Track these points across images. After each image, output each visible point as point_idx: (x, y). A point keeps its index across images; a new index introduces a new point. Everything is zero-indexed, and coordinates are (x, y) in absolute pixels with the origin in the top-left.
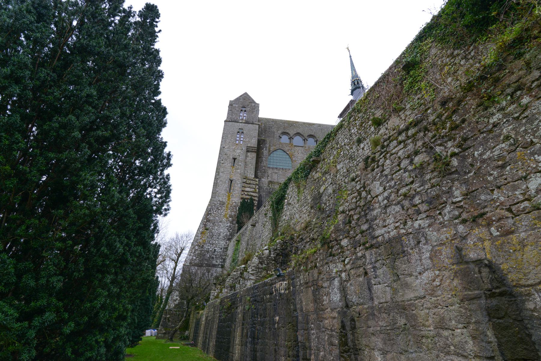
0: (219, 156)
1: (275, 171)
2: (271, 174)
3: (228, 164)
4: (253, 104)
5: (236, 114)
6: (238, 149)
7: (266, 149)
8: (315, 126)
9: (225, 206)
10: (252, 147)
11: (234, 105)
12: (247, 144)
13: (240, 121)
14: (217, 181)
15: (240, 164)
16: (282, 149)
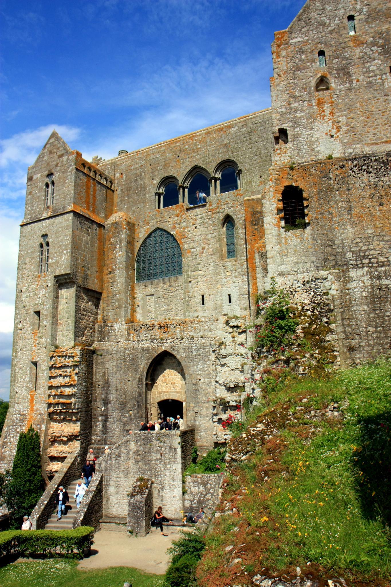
0: (16, 314)
1: (150, 289)
2: (142, 300)
3: (28, 330)
5: (38, 197)
6: (41, 288)
7: (120, 247)
8: (232, 130)
9: (26, 423)
10: (62, 275)
11: (35, 178)
12: (55, 270)
13: (45, 215)
14: (15, 370)
15: (45, 323)
16: (161, 226)
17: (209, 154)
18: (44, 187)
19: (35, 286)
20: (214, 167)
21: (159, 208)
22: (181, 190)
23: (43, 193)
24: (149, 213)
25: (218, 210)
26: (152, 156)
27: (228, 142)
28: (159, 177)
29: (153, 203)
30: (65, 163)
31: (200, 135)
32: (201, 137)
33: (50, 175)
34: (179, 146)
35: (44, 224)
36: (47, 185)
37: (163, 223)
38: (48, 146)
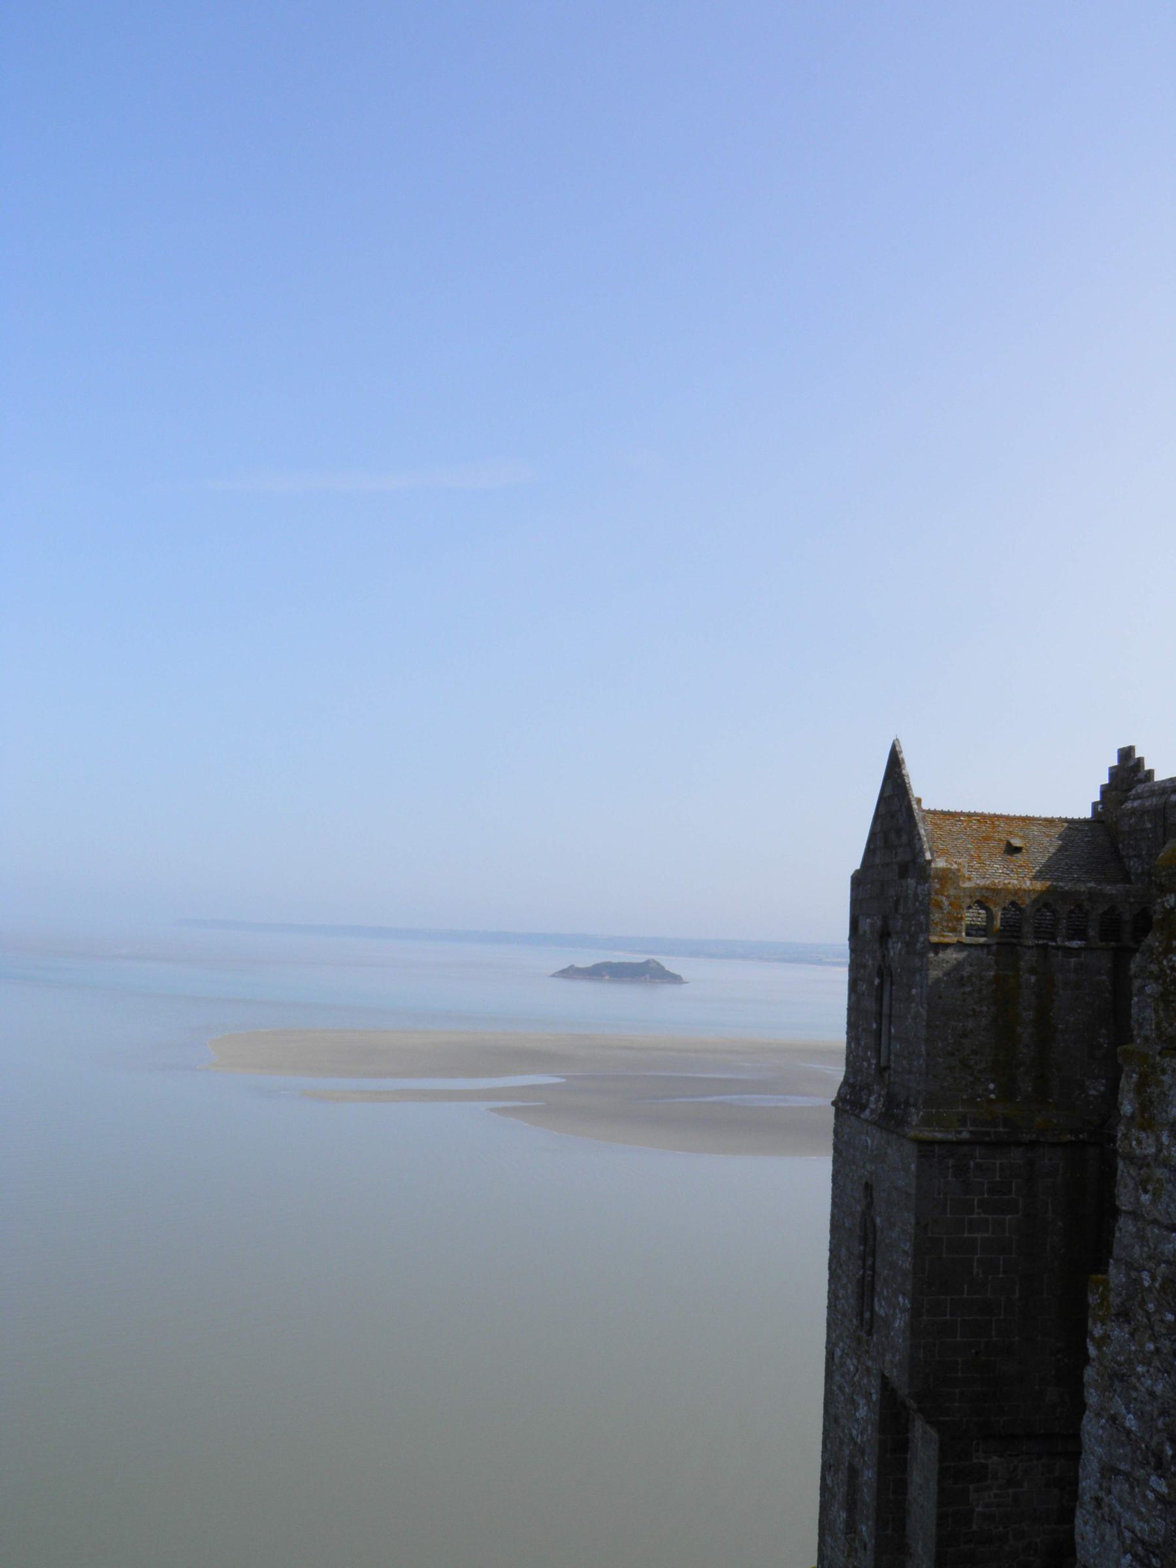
4: (911, 882)
18: (877, 981)
19: (852, 1368)
33: (884, 935)
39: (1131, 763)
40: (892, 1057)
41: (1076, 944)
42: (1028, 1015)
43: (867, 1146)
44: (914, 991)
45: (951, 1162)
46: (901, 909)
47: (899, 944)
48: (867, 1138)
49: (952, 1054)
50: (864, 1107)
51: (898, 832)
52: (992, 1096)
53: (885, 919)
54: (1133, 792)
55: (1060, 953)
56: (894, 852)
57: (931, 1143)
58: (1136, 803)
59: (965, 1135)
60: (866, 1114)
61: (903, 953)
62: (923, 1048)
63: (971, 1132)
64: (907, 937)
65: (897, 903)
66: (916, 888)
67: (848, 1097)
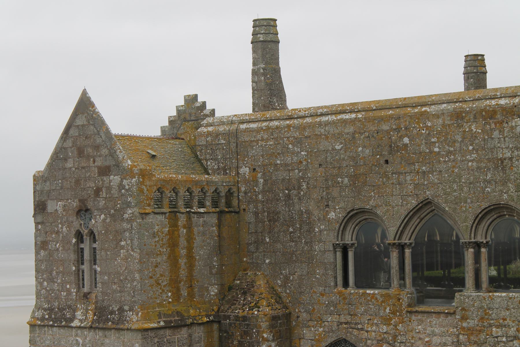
4: (115, 179)
16: (351, 339)
17: (460, 177)
18: (74, 241)
20: (471, 218)
21: (346, 284)
22: (394, 255)
23: (73, 256)
24: (322, 295)
25: (482, 336)
26: (324, 145)
27: (508, 155)
28: (342, 205)
29: (330, 272)
30: (115, 192)
31: (437, 116)
32: (440, 121)
34: (388, 132)
35: (80, 341)
36: (79, 236)
37: (355, 332)
38: (72, 132)
39: (198, 105)
40: (99, 285)
41: (202, 210)
42: (184, 252)
43: (78, 343)
44: (123, 243)
45: (156, 340)
46: (103, 194)
47: (103, 216)
48: (79, 339)
49: (151, 278)
50: (72, 320)
51: (97, 148)
52: (170, 300)
53: (82, 201)
54: (205, 122)
55: (196, 216)
56: (92, 160)
57: (146, 330)
58: (210, 129)
59: (162, 324)
60: (76, 323)
61: (108, 220)
62: (137, 276)
63: (164, 321)
64: (112, 211)
65: (97, 192)
66: (122, 181)
67: (47, 316)
